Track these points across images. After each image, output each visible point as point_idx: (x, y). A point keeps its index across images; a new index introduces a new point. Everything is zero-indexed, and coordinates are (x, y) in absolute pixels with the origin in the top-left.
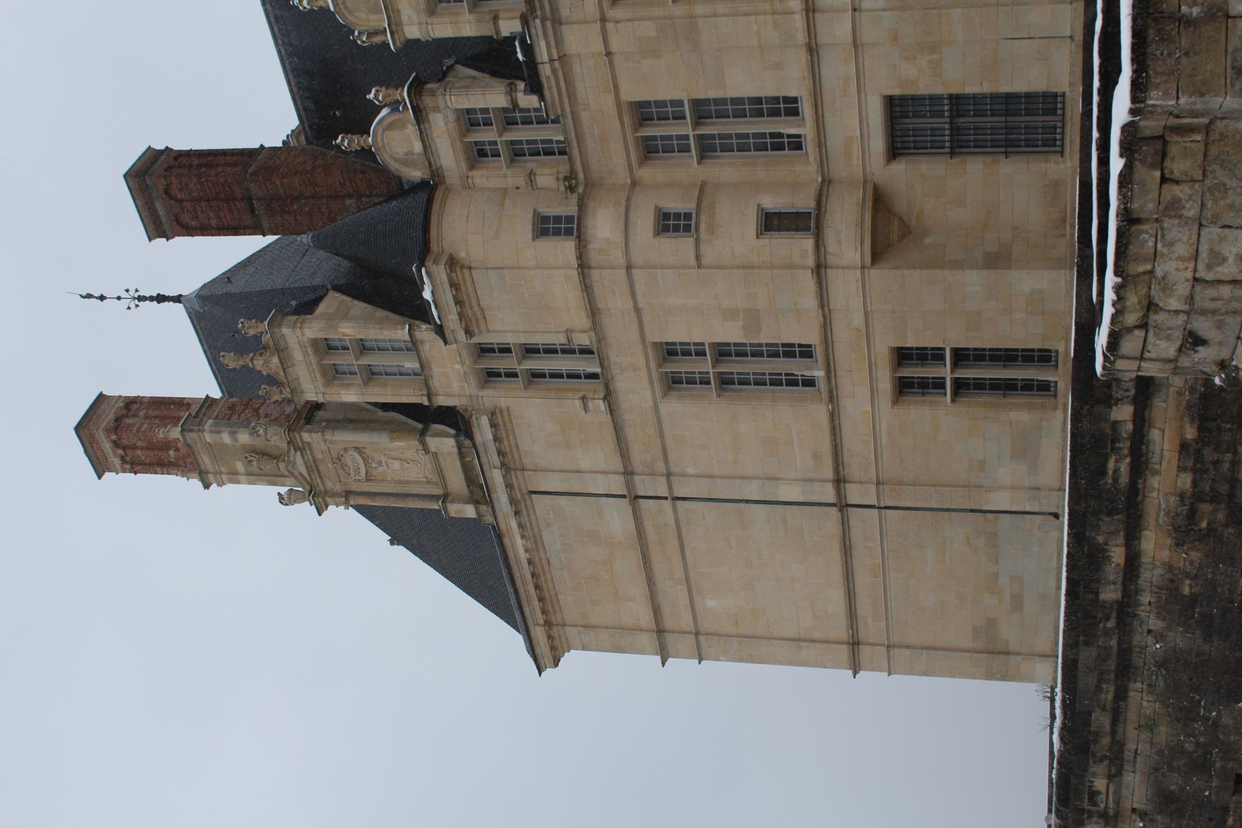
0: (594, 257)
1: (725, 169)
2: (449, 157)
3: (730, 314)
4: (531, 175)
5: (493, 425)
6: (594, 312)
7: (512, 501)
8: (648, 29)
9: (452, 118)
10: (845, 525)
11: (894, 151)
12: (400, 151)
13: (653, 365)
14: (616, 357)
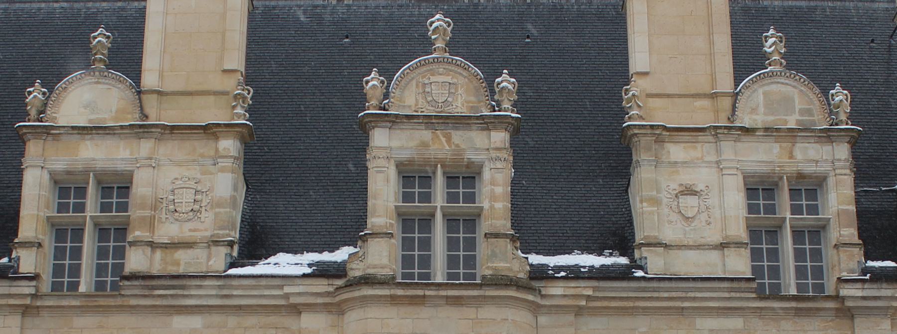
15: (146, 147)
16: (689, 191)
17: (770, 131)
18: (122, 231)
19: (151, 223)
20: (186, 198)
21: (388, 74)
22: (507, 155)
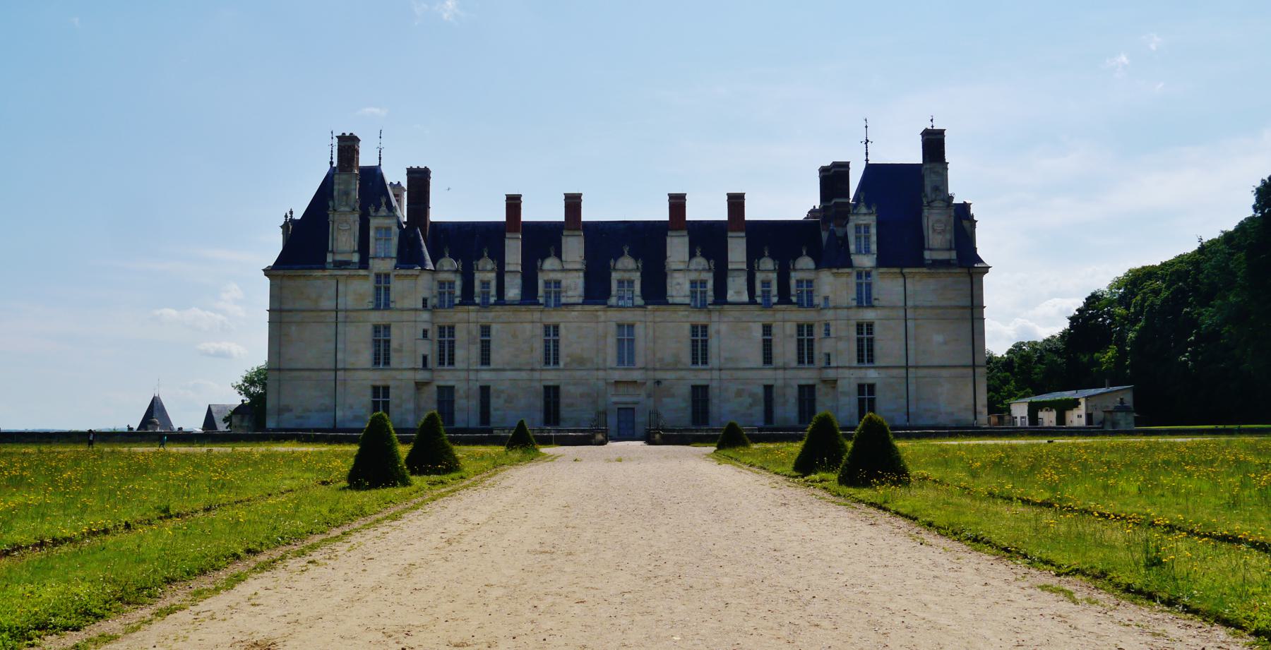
0: (418, 312)
1: (436, 347)
2: (443, 276)
3: (401, 345)
4: (435, 297)
5: (364, 275)
6: (402, 310)
7: (336, 275)
8: (474, 333)
9: (454, 279)
10: (330, 370)
11: (439, 387)
12: (445, 264)
13: (384, 323)
14: (386, 313)
15: (564, 274)
16: (679, 284)
17: (696, 270)
18: (559, 292)
19: (566, 292)
20: (573, 286)
21: (616, 260)
22: (640, 278)
